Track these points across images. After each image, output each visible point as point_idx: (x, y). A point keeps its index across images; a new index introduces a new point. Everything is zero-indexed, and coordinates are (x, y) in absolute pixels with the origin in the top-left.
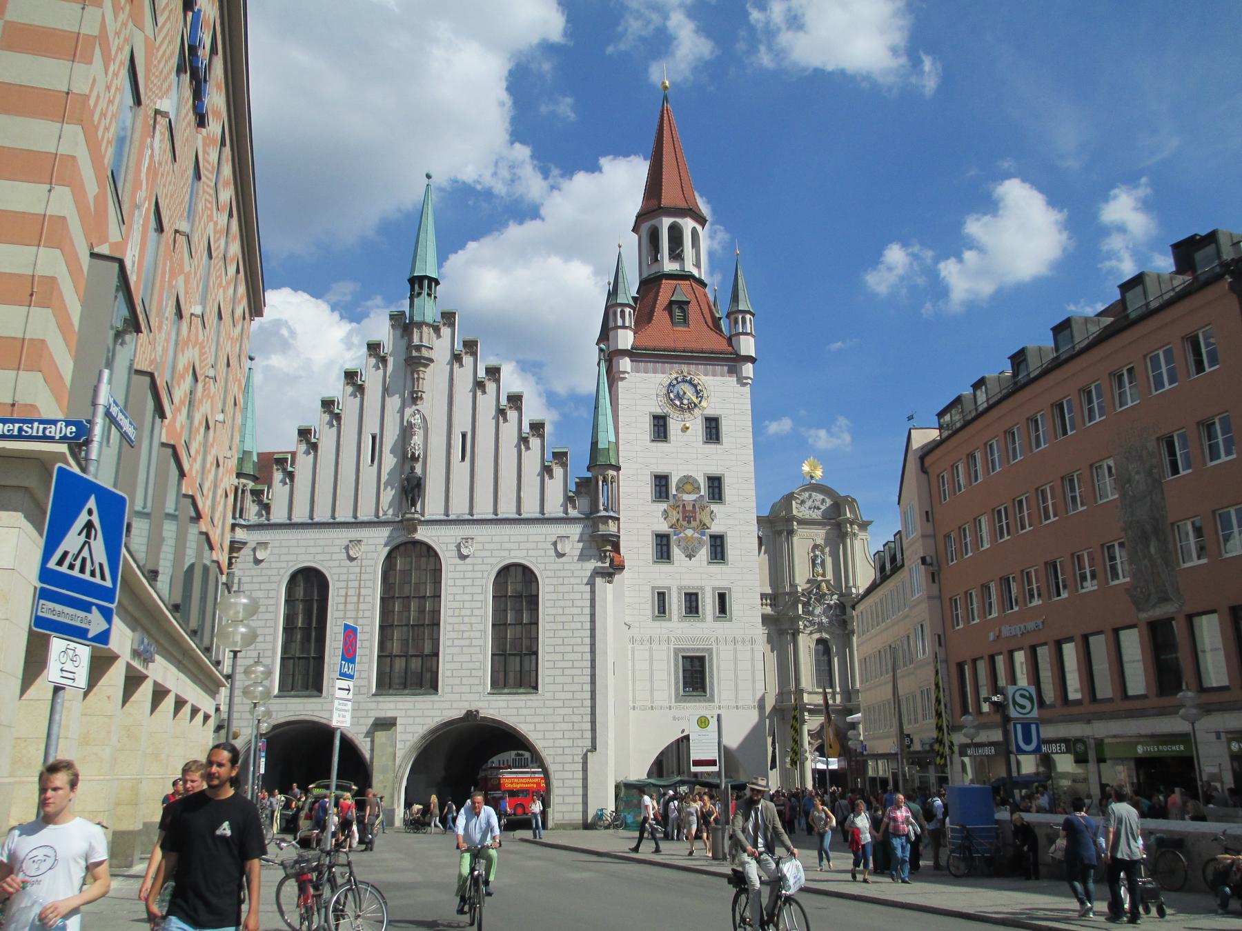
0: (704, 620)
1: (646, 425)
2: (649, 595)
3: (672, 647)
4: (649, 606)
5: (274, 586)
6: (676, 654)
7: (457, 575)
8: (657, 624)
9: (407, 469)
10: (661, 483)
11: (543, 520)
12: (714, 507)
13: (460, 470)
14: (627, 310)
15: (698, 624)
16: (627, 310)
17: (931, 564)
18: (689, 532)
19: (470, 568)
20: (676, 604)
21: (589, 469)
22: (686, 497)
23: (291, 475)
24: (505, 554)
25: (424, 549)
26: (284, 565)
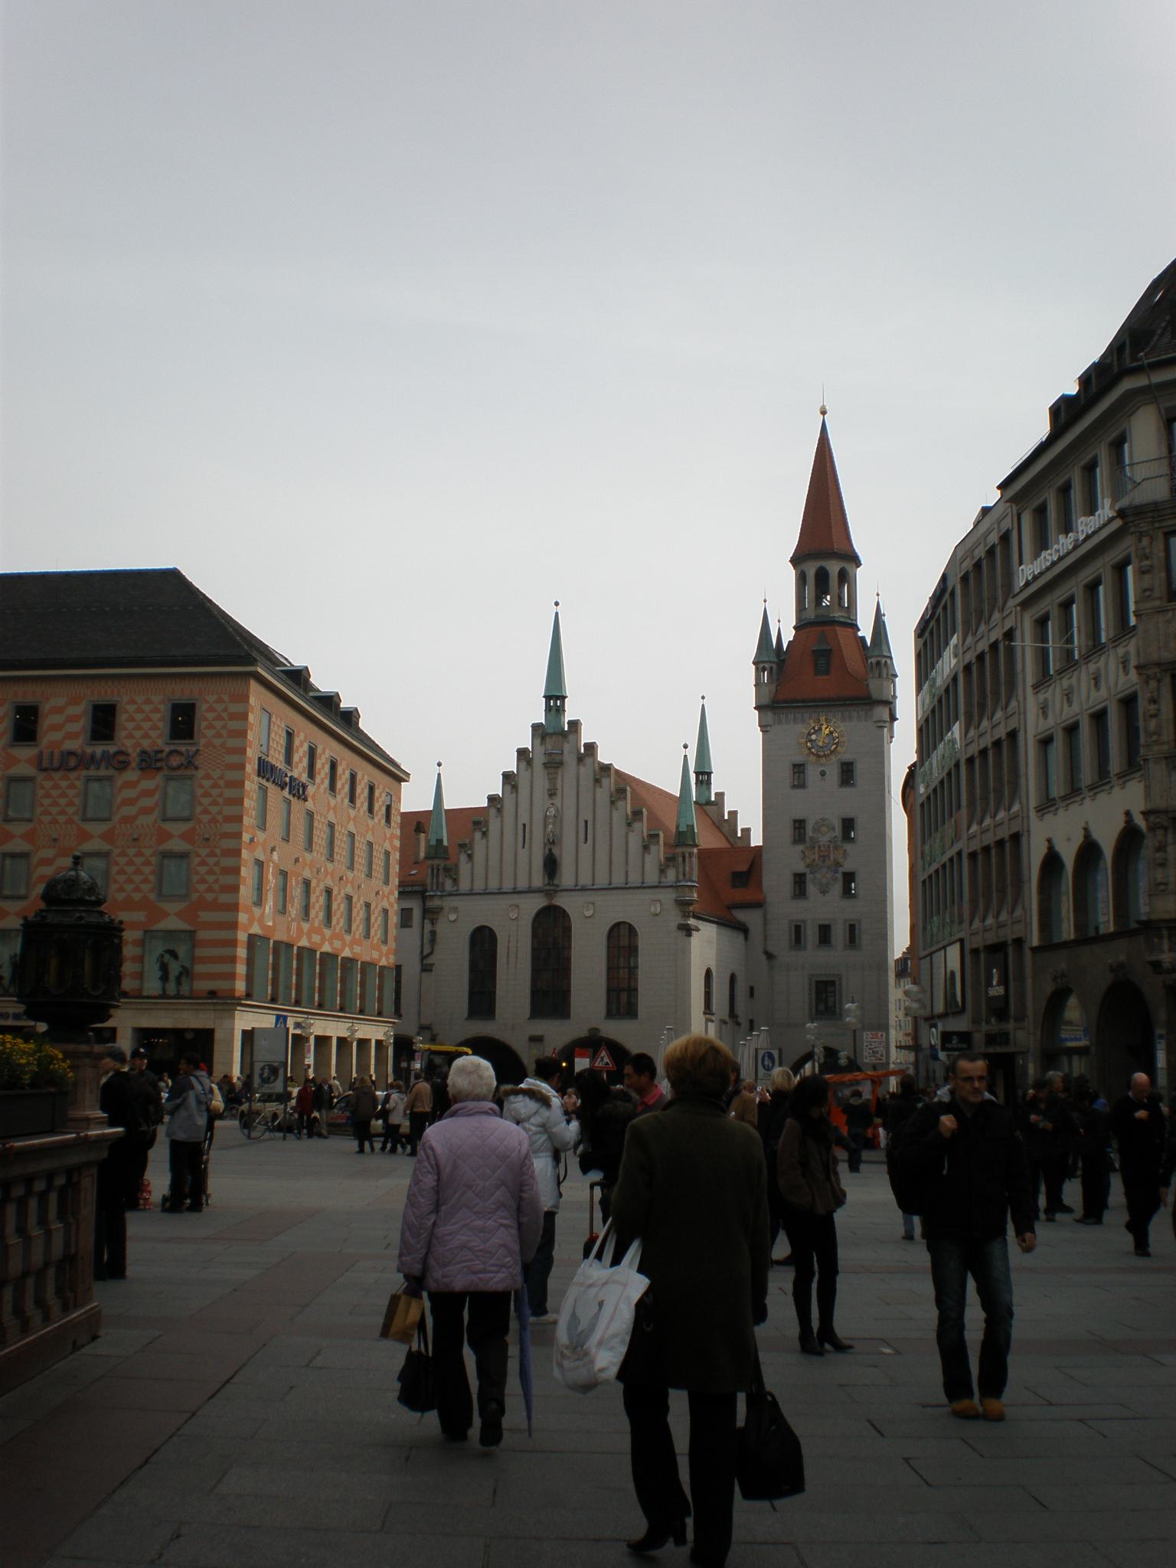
11: (642, 887)
12: (848, 847)
13: (586, 849)
20: (811, 935)
23: (470, 857)
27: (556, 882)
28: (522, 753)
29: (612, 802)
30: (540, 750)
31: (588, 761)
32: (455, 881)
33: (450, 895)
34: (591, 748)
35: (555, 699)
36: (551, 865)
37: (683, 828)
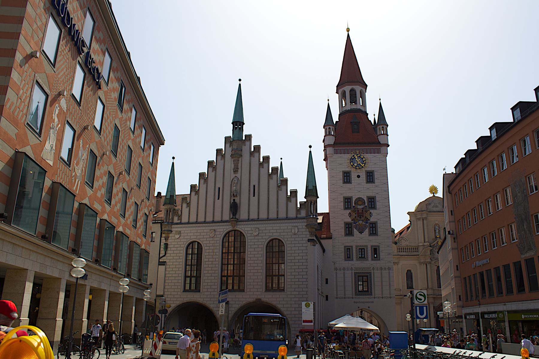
0: (367, 260)
1: (341, 176)
2: (343, 250)
3: (353, 272)
4: (343, 254)
5: (182, 249)
6: (355, 275)
7: (252, 243)
8: (347, 262)
9: (232, 201)
10: (347, 200)
12: (372, 211)
13: (254, 200)
14: (331, 127)
15: (365, 262)
16: (331, 127)
17: (453, 234)
18: (361, 222)
19: (257, 240)
21: (305, 197)
22: (359, 207)
24: (271, 234)
25: (239, 233)
26: (186, 240)
27: (237, 217)
28: (219, 151)
29: (269, 175)
30: (229, 150)
31: (256, 155)
32: (180, 217)
33: (177, 224)
34: (258, 148)
35: (238, 124)
36: (234, 208)
37: (311, 187)
